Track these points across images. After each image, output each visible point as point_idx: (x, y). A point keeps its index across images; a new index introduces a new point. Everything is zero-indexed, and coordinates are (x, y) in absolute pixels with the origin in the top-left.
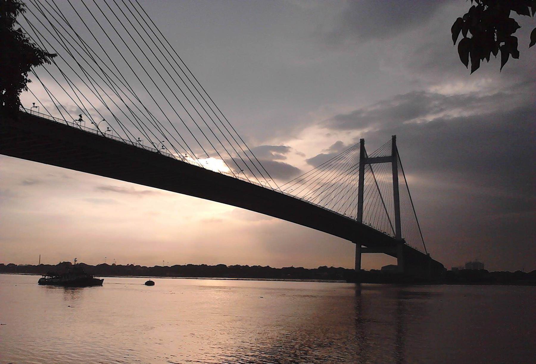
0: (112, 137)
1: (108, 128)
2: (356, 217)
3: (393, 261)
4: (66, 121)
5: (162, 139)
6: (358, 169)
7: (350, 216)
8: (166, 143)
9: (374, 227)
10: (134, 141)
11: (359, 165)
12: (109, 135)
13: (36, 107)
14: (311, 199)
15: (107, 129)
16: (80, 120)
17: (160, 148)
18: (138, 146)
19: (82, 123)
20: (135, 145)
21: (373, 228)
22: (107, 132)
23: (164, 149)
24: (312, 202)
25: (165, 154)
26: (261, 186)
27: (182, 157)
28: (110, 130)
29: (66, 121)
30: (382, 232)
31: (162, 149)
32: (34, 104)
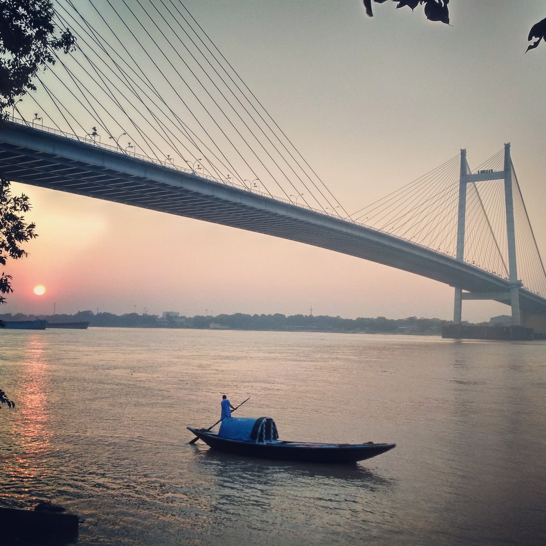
0: (134, 155)
1: (129, 143)
2: (455, 253)
3: (506, 310)
4: (77, 136)
5: (199, 155)
6: (458, 188)
8: (204, 162)
10: (163, 159)
11: (459, 183)
12: (131, 153)
13: (40, 119)
14: (392, 230)
15: (128, 145)
16: (94, 134)
17: (195, 168)
18: (167, 166)
19: (97, 139)
20: (164, 165)
21: (478, 266)
22: (129, 149)
24: (394, 233)
25: (201, 176)
26: (325, 214)
27: (223, 179)
28: (132, 147)
29: (77, 136)
30: (491, 272)
32: (36, 115)
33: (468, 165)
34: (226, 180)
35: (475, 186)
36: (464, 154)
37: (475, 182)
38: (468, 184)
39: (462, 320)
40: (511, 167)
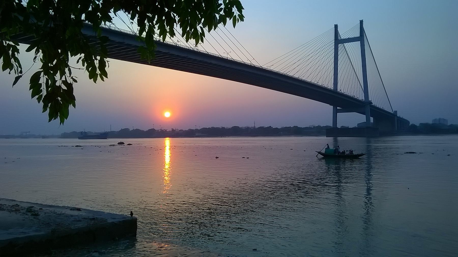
7: (327, 86)
9: (348, 94)
21: (347, 94)
23: (179, 42)
27: (193, 47)
31: (178, 42)
33: (339, 34)
34: (195, 48)
35: (344, 45)
36: (336, 27)
37: (344, 44)
38: (339, 45)
39: (339, 126)
40: (364, 33)
